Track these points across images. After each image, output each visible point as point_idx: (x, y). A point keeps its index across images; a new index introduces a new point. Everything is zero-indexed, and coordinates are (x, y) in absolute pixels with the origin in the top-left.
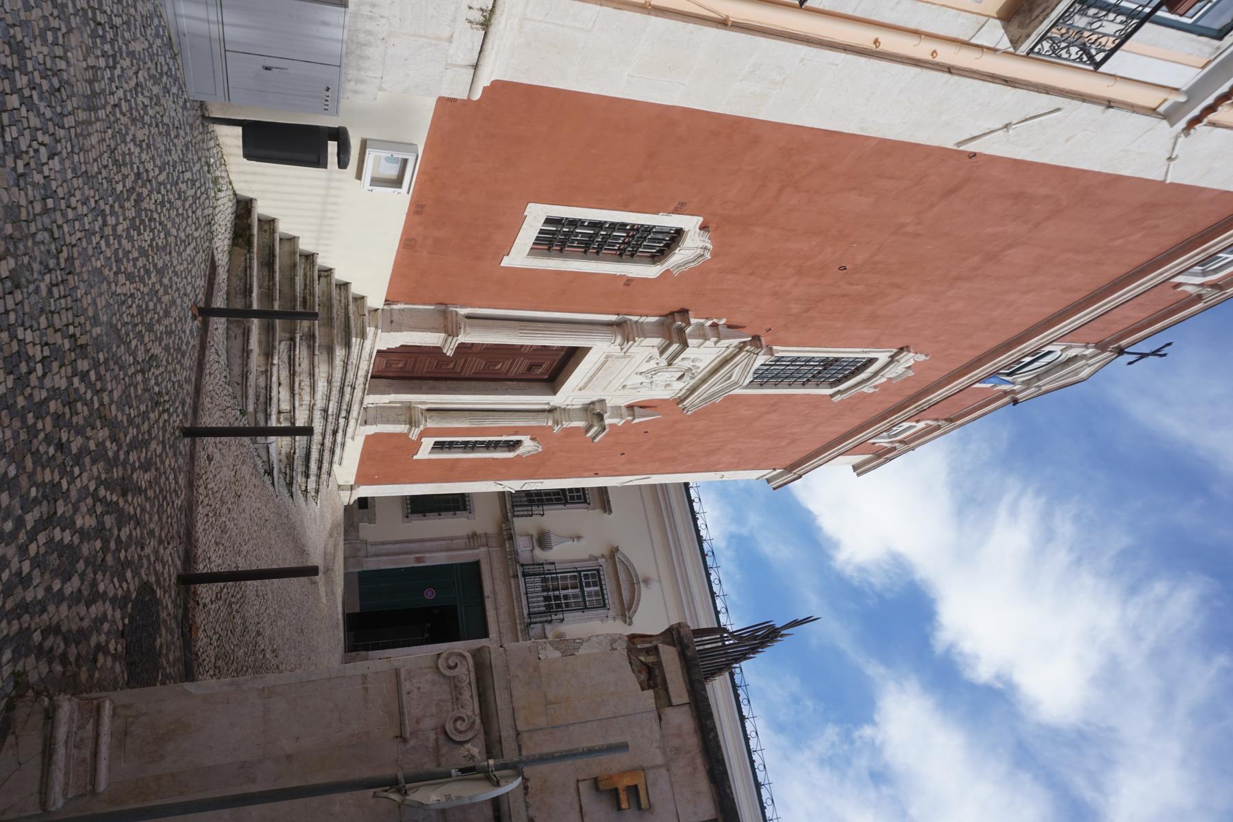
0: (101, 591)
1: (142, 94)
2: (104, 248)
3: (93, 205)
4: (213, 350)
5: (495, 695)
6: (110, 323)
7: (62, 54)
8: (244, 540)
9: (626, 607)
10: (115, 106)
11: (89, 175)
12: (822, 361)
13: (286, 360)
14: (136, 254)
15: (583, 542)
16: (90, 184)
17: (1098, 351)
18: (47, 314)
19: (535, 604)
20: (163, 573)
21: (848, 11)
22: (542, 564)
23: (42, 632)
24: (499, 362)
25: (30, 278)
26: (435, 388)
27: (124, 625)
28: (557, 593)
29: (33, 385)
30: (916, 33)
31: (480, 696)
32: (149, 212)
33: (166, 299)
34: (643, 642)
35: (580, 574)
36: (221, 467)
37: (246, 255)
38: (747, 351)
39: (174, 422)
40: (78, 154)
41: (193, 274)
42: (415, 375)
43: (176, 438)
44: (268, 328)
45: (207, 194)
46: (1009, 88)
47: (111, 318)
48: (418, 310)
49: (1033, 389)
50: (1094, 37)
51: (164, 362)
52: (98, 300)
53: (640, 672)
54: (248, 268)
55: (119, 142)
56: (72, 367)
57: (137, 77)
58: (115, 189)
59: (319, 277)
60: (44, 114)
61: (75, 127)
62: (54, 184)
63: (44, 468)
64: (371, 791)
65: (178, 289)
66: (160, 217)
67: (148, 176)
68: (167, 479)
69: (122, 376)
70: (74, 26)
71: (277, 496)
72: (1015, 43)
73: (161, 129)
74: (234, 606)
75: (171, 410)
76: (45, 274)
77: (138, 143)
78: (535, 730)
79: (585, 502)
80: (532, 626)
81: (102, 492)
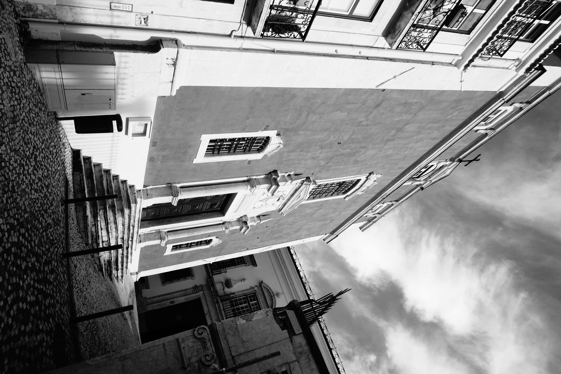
1: (32, 113)
2: (25, 180)
4: (71, 218)
8: (94, 302)
10: (22, 120)
12: (338, 184)
13: (103, 218)
14: (37, 181)
15: (246, 281)
16: (17, 154)
17: (451, 162)
19: (229, 314)
20: (64, 319)
22: (229, 294)
24: (198, 206)
26: (170, 221)
27: (51, 342)
29: (5, 241)
31: (214, 344)
33: (51, 198)
36: (81, 270)
38: (305, 184)
42: (160, 217)
45: (61, 150)
48: (159, 188)
49: (429, 182)
50: (421, 39)
51: (53, 226)
53: (280, 323)
55: (26, 134)
57: (29, 106)
59: (113, 179)
61: (9, 131)
65: (55, 193)
67: (38, 147)
68: (60, 277)
69: (38, 234)
70: (4, 90)
71: (105, 281)
72: (391, 45)
73: (40, 126)
74: (94, 332)
75: (58, 246)
78: (240, 355)
81: (36, 285)
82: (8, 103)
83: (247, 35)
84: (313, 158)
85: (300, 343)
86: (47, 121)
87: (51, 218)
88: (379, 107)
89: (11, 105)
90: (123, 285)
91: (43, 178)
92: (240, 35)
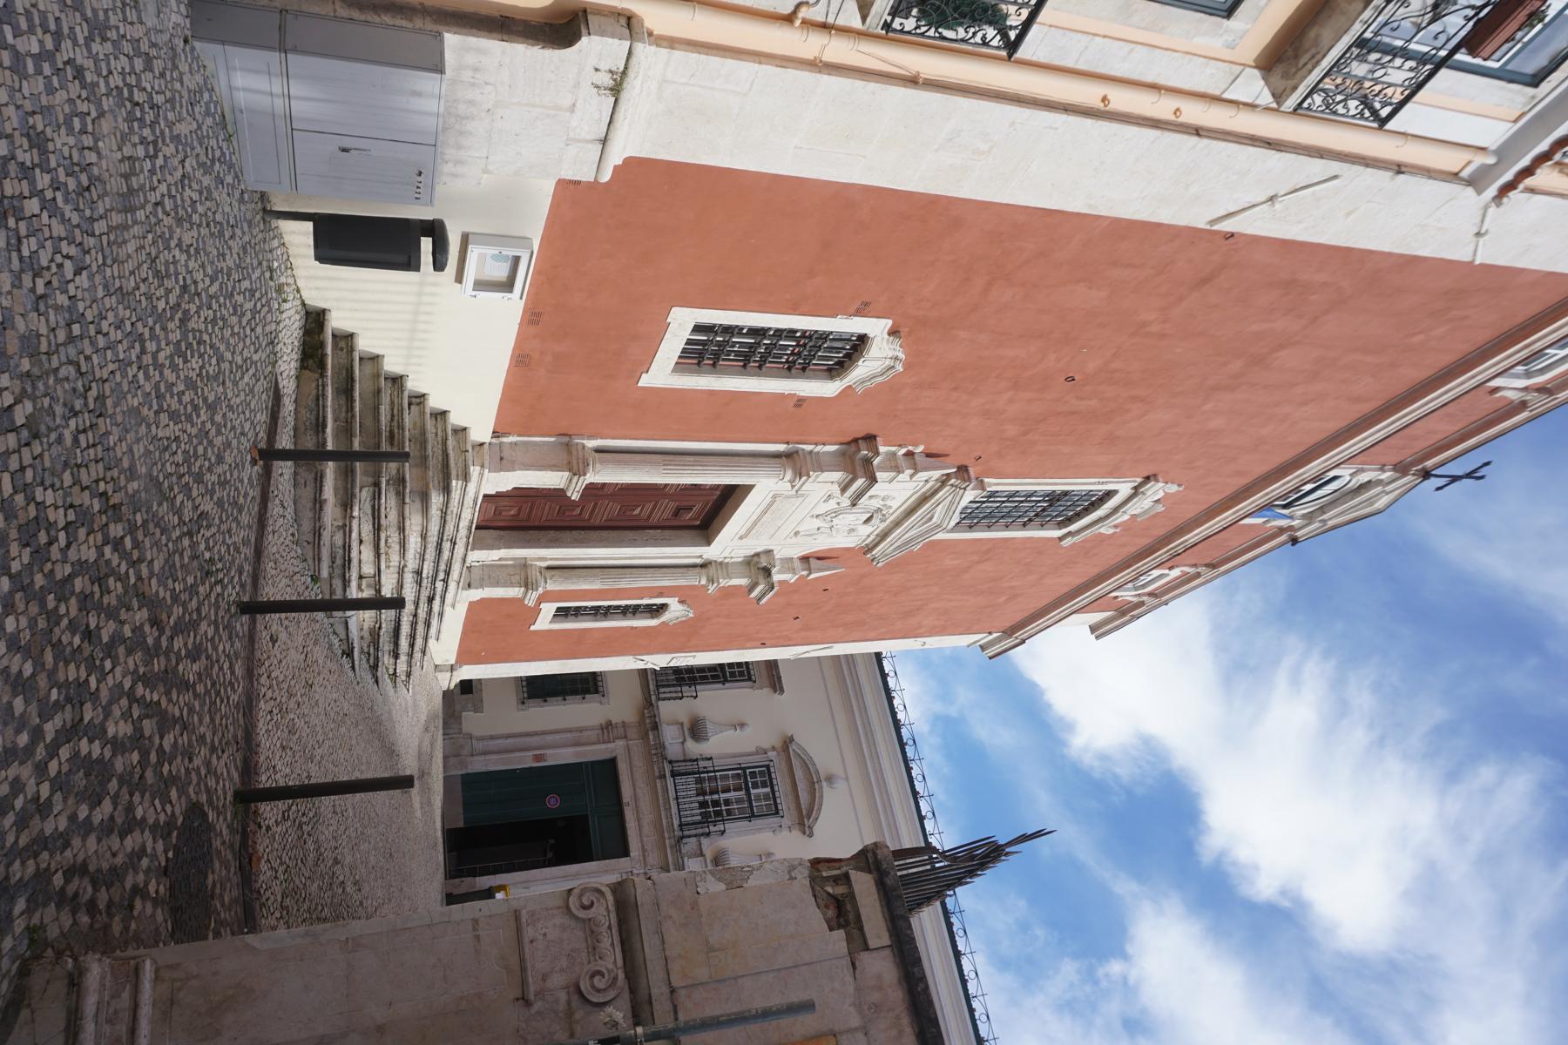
0: (139, 818)
1: (190, 187)
2: (142, 382)
4: (277, 501)
5: (642, 942)
6: (150, 476)
7: (91, 144)
8: (318, 742)
9: (804, 813)
10: (157, 204)
11: (125, 291)
13: (369, 511)
14: (181, 387)
15: (748, 730)
16: (126, 302)
17: (1398, 475)
18: (72, 469)
19: (688, 812)
21: (1069, 63)
22: (696, 760)
23: (64, 873)
25: (51, 425)
26: (557, 540)
27: (167, 859)
28: (715, 797)
30: (1155, 87)
31: (623, 943)
32: (198, 334)
33: (218, 441)
34: (829, 869)
35: (745, 773)
36: (288, 649)
37: (318, 380)
38: (952, 485)
41: (252, 407)
42: (531, 524)
43: (231, 616)
44: (346, 472)
46: (1274, 152)
47: (151, 468)
48: (535, 443)
49: (1316, 525)
50: (1378, 88)
51: (217, 521)
53: (827, 907)
54: (320, 397)
55: (161, 249)
56: (103, 534)
57: (183, 167)
59: (410, 404)
60: (70, 219)
61: (107, 234)
62: (81, 306)
63: (67, 663)
65: (233, 428)
66: (211, 339)
67: (196, 288)
68: (221, 668)
69: (164, 542)
70: (106, 108)
71: (358, 683)
72: (1279, 97)
73: (213, 230)
74: (305, 827)
75: (226, 581)
76: (69, 418)
77: (185, 248)
79: (750, 679)
80: (685, 840)
81: (140, 690)
82: (115, 148)
83: (841, 22)
86: (235, 217)
87: (212, 499)
90: (409, 697)
91: (202, 381)
92: (820, 18)
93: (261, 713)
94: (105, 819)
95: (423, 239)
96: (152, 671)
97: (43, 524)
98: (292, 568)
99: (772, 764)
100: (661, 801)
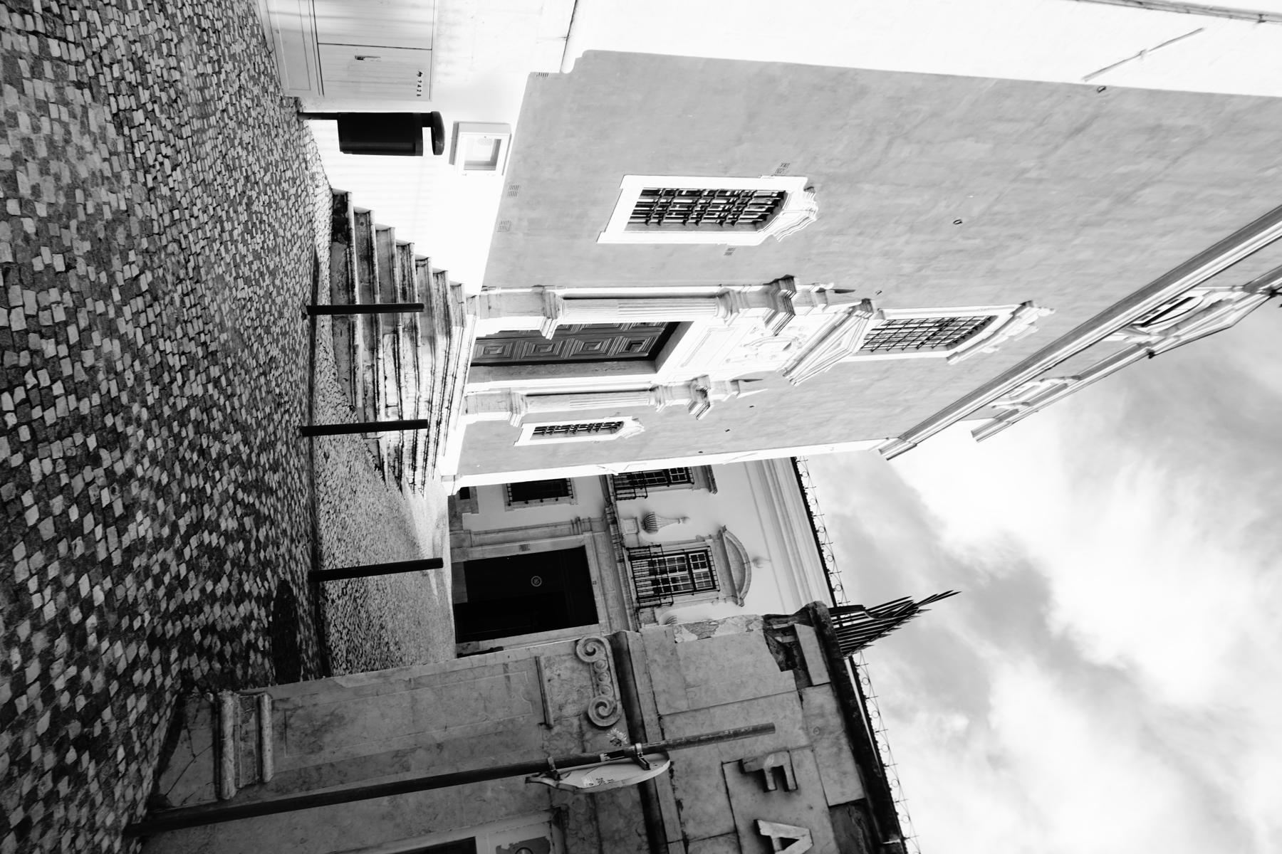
0: (247, 591)
1: (245, 96)
2: (224, 255)
3: (212, 213)
4: (322, 348)
5: (635, 680)
7: (176, 65)
9: (737, 587)
10: (223, 111)
12: (938, 322)
13: (391, 354)
14: (250, 258)
15: (689, 522)
17: (1246, 294)
19: (643, 588)
20: (296, 571)
22: (649, 547)
23: (200, 631)
25: (165, 290)
26: (534, 373)
27: (269, 622)
31: (619, 681)
32: (259, 215)
33: (279, 300)
34: (779, 623)
35: (688, 556)
38: (857, 316)
39: (294, 422)
40: (196, 163)
42: (513, 360)
44: (372, 322)
45: (306, 191)
46: (1145, 10)
47: (235, 323)
48: (516, 294)
51: (282, 364)
52: (223, 306)
53: (778, 652)
54: (348, 263)
57: (240, 80)
58: (228, 194)
59: (417, 266)
60: (165, 127)
61: (191, 137)
62: (178, 195)
63: (190, 475)
64: (522, 778)
65: (288, 289)
67: (255, 179)
68: (293, 479)
69: (248, 380)
70: (183, 35)
74: (358, 600)
75: (291, 410)
76: (177, 284)
77: (245, 146)
79: (689, 481)
80: (641, 610)
81: (240, 495)
82: (192, 67)
84: (886, 254)
85: (822, 707)
86: (278, 119)
87: (277, 346)
88: (1080, 135)
89: (198, 74)
91: (264, 252)
93: (321, 514)
94: (225, 591)
95: (424, 129)
96: (247, 480)
97: (166, 368)
98: (336, 401)
99: (709, 549)
100: (621, 580)
